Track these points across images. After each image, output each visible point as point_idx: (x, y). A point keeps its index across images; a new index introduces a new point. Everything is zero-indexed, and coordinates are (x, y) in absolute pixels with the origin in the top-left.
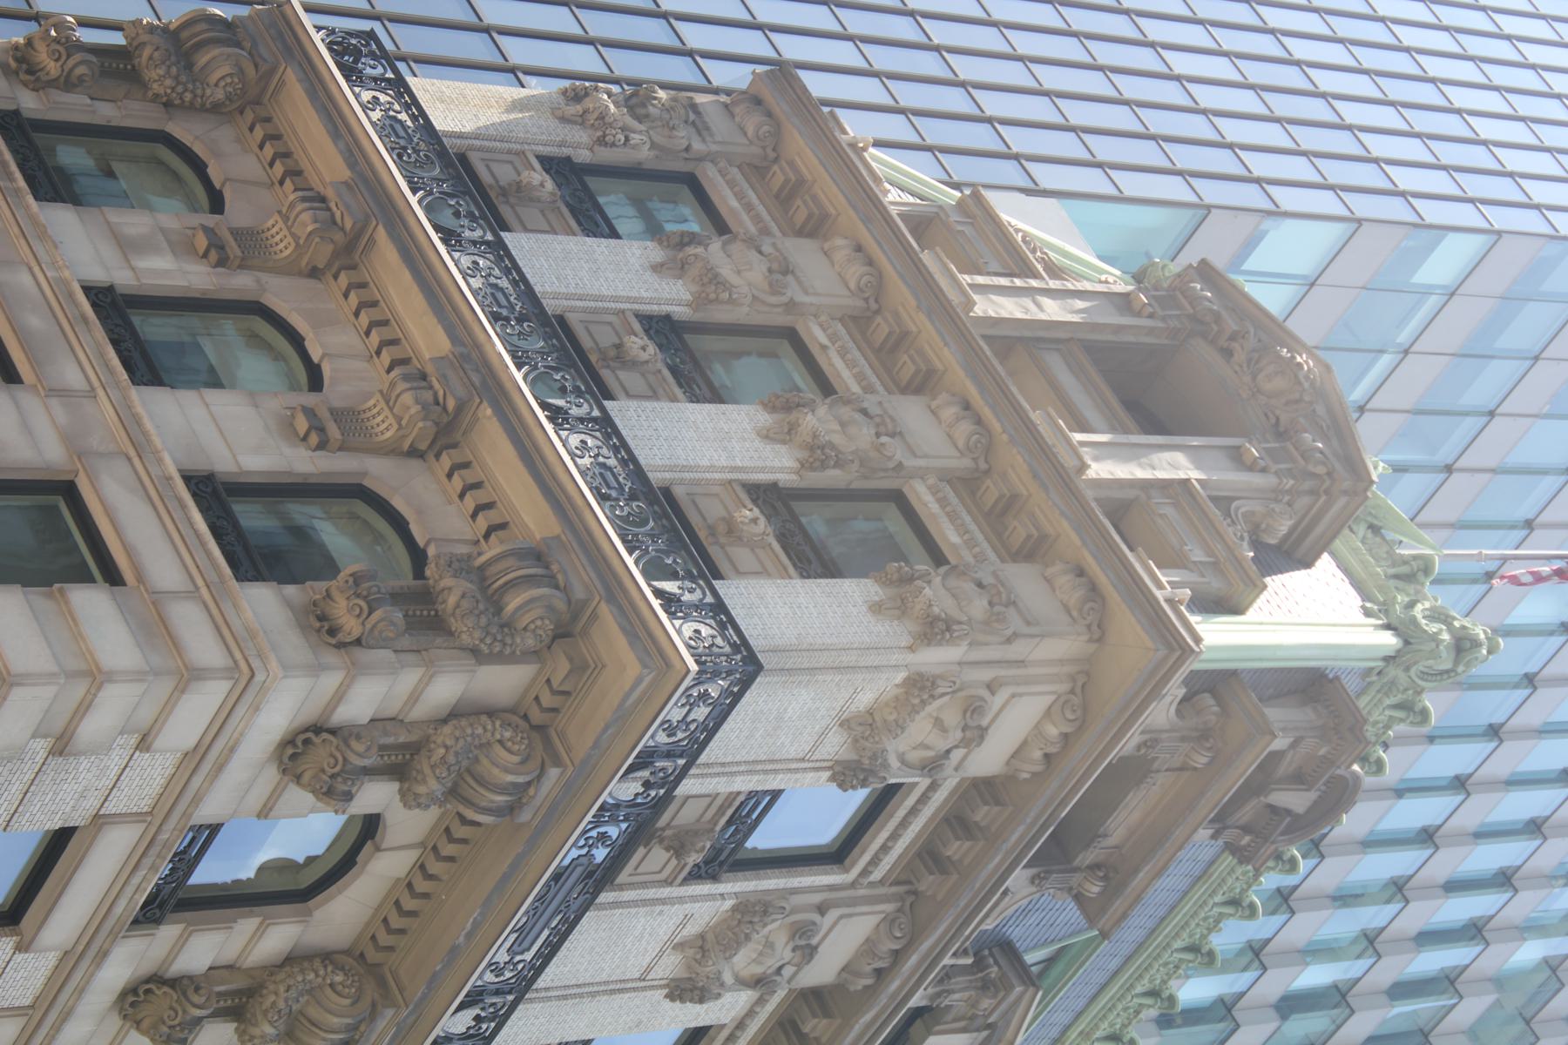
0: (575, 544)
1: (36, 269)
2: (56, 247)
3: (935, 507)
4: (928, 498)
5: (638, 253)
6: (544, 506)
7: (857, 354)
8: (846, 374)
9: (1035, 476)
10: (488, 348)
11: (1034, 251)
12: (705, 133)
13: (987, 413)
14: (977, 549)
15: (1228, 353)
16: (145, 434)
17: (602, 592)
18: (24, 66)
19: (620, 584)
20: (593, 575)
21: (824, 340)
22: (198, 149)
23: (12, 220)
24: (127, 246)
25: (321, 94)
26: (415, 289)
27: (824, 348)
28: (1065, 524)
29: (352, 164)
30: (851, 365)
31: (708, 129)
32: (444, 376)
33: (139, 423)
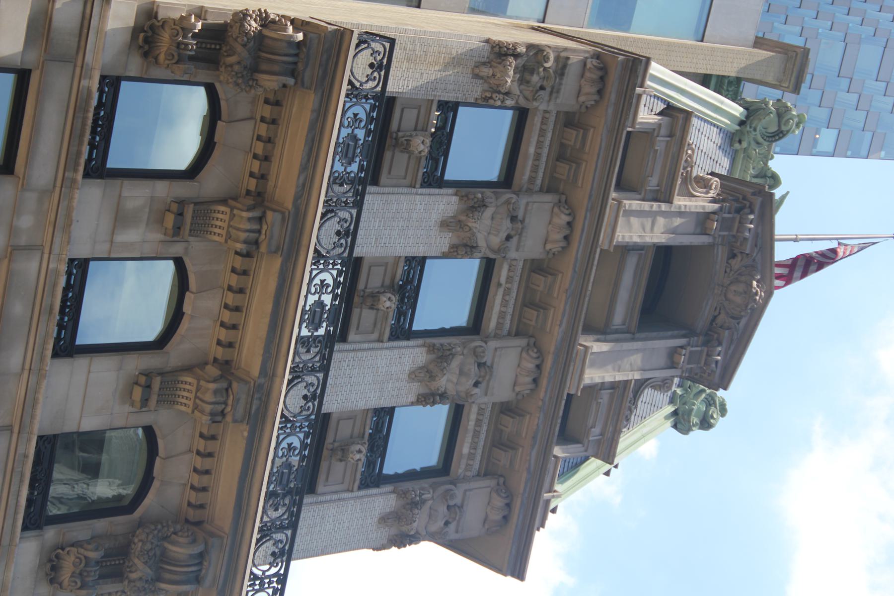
0: (227, 549)
1: (46, 256)
2: (68, 243)
3: (472, 424)
4: (473, 416)
5: (442, 207)
7: (512, 302)
8: (497, 308)
9: (534, 438)
10: (278, 380)
11: (684, 168)
12: (554, 95)
13: (544, 382)
14: (471, 462)
15: (734, 256)
16: (33, 417)
17: (220, 587)
18: (146, 47)
20: (223, 573)
21: (503, 280)
23: (55, 208)
24: (121, 219)
25: (319, 125)
26: (266, 320)
28: (525, 475)
29: (297, 197)
30: (504, 303)
31: (558, 92)
32: (238, 400)
33: (34, 407)
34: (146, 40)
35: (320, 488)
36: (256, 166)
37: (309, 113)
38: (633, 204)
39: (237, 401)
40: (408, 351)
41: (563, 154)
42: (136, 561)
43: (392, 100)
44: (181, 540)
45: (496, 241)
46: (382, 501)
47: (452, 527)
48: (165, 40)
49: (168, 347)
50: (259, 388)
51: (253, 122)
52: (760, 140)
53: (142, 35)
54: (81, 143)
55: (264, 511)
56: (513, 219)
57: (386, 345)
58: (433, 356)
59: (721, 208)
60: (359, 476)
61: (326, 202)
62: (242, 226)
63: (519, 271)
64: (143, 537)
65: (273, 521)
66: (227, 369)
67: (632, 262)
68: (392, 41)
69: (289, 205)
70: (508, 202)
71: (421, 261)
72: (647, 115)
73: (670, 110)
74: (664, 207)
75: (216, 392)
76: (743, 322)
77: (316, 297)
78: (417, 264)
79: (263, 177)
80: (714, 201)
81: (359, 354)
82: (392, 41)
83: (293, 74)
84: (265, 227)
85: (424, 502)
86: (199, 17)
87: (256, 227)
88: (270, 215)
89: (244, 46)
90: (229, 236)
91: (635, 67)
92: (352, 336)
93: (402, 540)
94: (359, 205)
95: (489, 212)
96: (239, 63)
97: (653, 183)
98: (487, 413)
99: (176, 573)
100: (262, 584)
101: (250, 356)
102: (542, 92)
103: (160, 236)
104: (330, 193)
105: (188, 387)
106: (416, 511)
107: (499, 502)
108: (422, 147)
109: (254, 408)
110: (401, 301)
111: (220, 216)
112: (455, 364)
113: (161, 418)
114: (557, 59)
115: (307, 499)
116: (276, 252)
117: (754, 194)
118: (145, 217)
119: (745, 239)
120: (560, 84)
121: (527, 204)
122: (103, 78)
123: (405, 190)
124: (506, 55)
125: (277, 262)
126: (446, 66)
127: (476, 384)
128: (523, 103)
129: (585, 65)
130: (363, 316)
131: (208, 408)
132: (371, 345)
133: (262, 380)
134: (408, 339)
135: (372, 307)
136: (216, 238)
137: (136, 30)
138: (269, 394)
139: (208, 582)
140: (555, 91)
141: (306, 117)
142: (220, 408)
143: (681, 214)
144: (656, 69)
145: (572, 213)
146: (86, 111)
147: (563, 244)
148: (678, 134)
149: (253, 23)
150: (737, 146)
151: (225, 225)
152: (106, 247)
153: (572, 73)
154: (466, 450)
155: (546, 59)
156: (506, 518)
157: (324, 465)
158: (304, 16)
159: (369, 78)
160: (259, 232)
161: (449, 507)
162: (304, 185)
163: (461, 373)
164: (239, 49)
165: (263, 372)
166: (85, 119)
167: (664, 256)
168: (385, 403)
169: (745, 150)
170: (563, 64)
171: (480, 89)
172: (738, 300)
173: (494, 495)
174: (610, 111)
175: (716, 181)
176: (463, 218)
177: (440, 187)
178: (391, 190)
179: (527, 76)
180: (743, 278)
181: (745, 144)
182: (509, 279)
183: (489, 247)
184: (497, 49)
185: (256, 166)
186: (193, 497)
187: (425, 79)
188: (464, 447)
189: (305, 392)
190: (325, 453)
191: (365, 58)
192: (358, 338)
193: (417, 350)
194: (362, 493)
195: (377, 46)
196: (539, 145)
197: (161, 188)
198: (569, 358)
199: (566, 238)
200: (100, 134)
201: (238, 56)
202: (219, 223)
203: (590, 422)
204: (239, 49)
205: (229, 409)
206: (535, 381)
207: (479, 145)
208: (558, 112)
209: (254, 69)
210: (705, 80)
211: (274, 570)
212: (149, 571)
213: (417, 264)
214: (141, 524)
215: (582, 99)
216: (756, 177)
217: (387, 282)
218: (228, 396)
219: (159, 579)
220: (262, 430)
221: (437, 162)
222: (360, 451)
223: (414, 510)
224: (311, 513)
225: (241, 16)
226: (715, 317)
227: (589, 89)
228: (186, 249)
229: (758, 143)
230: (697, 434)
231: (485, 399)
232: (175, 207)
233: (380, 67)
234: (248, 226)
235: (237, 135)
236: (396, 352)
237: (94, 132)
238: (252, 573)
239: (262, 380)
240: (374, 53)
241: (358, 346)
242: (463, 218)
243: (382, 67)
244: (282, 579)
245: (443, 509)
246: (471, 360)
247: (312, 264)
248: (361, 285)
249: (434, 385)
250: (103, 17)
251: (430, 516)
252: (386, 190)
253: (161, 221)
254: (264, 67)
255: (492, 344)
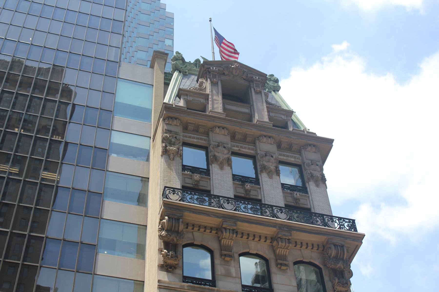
3: (284, 158)
4: (282, 157)
5: (216, 169)
6: (317, 236)
7: (244, 145)
9: (288, 137)
10: (277, 222)
13: (270, 134)
15: (224, 74)
18: (173, 268)
19: (340, 234)
21: (238, 149)
22: (186, 243)
24: (228, 275)
25: (194, 211)
26: (258, 226)
27: (239, 150)
31: (176, 132)
32: (284, 235)
34: (171, 268)
35: (309, 207)
36: (208, 231)
37: (191, 214)
38: (210, 107)
39: (285, 235)
40: (263, 179)
41: (196, 130)
42: (337, 266)
43: (183, 187)
44: (330, 252)
45: (226, 151)
46: (311, 186)
47: (318, 163)
48: (169, 262)
49: (268, 258)
50: (280, 228)
51: (194, 232)
52: (185, 66)
53: (169, 269)
54: (205, 288)
55: (319, 225)
56: (218, 146)
57: (261, 187)
58: (264, 171)
59: (209, 78)
60: (304, 194)
61: (218, 208)
62: (228, 235)
63: (235, 143)
64: (330, 264)
65: (322, 222)
66: (273, 239)
67: (228, 107)
68: (165, 187)
69: (220, 220)
70: (213, 148)
71: (234, 176)
72: (181, 103)
73: (179, 96)
74: (210, 97)
75: (282, 242)
76: (245, 70)
77: (249, 210)
78: (235, 177)
79: (211, 228)
80: (207, 80)
81: (265, 195)
82: (165, 187)
83: (178, 220)
84: (228, 227)
85: (311, 173)
86: (162, 251)
87: (228, 231)
88: (224, 226)
89: (170, 236)
90: (231, 239)
91: (167, 107)
92: (260, 198)
93: (324, 180)
94: (218, 197)
95: (217, 154)
96: (176, 237)
97: (202, 101)
98: (281, 153)
99: (341, 254)
100: (342, 225)
101: (270, 231)
102: (177, 138)
103: (233, 261)
104: (216, 206)
105: (280, 251)
106: (314, 175)
107: (309, 148)
108: (198, 177)
109: (286, 229)
110: (247, 182)
111: (225, 242)
112: (266, 164)
113: (291, 260)
114: (166, 133)
115: (313, 211)
116: (236, 224)
117: (204, 68)
118: (227, 267)
119: (219, 70)
120: (174, 132)
121: (213, 141)
122: (183, 282)
123: (211, 182)
124: (166, 150)
125: (239, 223)
126: (171, 169)
127: (272, 157)
128: (181, 144)
129: (167, 124)
130: (253, 194)
131: (287, 244)
132: (262, 191)
133: (277, 227)
134: (259, 179)
135: (250, 192)
136: (232, 243)
137: (167, 271)
138: (282, 225)
139: (343, 243)
140: (176, 133)
141: (192, 215)
142: (287, 240)
143: (212, 91)
144: (166, 100)
145: (215, 127)
146: (195, 287)
147: (225, 129)
148: (186, 93)
149: (163, 233)
150: (187, 73)
151: (228, 240)
152: (237, 279)
153: (171, 128)
154: (293, 159)
155: (166, 136)
156: (314, 146)
157: (301, 206)
158: (158, 217)
159: (178, 194)
160: (230, 229)
161: (312, 165)
162: (214, 215)
163: (269, 162)
164: (171, 237)
165: (274, 227)
166: (197, 287)
167: (226, 96)
168: (280, 186)
169: (188, 71)
170: (168, 131)
171: (177, 158)
172: (238, 72)
173: (307, 150)
174: (182, 115)
175: (200, 80)
176: (219, 162)
177: (209, 170)
178: (212, 186)
179: (172, 143)
180: (231, 70)
181: (187, 71)
182: (237, 147)
183: (228, 154)
184: (164, 153)
185: (208, 231)
186: (315, 248)
187: (176, 176)
188: (292, 160)
189: (280, 213)
190: (297, 205)
191: (171, 196)
192: (260, 196)
193: (262, 176)
194: (309, 193)
195: (167, 192)
196: (194, 138)
197: (217, 262)
198: (260, 126)
199: (223, 128)
200: (201, 282)
201: (174, 238)
202: (227, 243)
203: (281, 119)
204: (171, 237)
205: (287, 238)
206: (270, 137)
207: (195, 158)
208: (183, 132)
209: (178, 232)
210: (167, 85)
211: (337, 221)
212: (341, 262)
213: (235, 177)
214: (325, 265)
215: (178, 124)
216: (196, 67)
217: (241, 187)
218: (283, 238)
219: (343, 259)
220: (293, 226)
221: (202, 171)
222: (296, 194)
223: (311, 174)
224: (318, 209)
225: (161, 237)
226: (244, 79)
227: (175, 122)
228: (236, 253)
229: (186, 66)
230: (280, 84)
231: (277, 153)
232: (223, 257)
233: (174, 191)
234: (228, 233)
235: (198, 238)
236: (264, 183)
237: (201, 284)
238: (339, 229)
239: (277, 227)
240: (169, 193)
241: (263, 196)
242: (219, 162)
243: (174, 190)
244: (340, 218)
245: (313, 167)
246: (264, 159)
247: (238, 211)
248: (243, 195)
249: (274, 170)
250: (164, 282)
251: (315, 171)
252: (212, 188)
253: (228, 261)
254: (177, 229)
255: (259, 152)
